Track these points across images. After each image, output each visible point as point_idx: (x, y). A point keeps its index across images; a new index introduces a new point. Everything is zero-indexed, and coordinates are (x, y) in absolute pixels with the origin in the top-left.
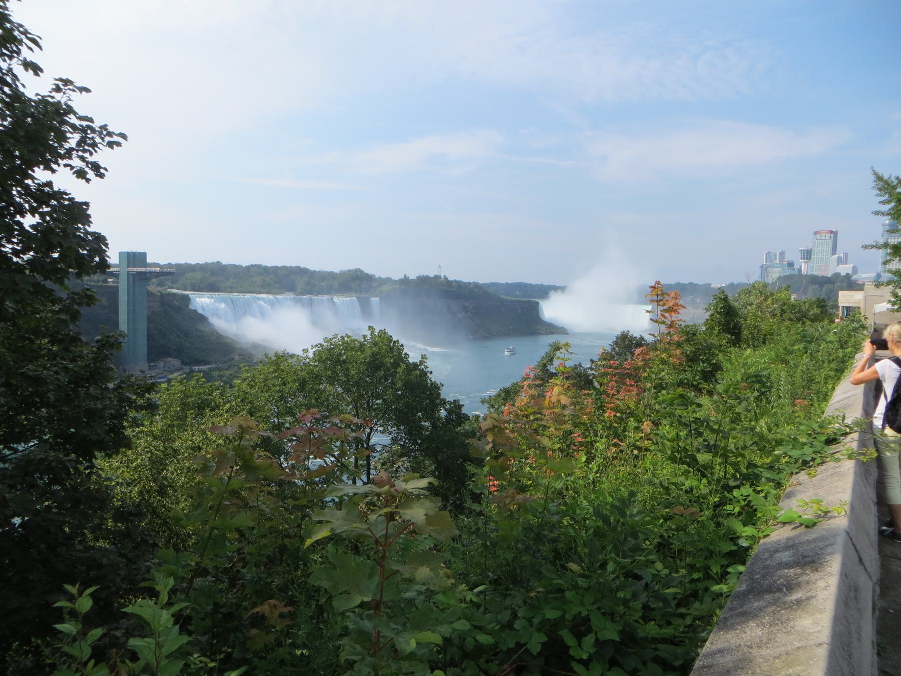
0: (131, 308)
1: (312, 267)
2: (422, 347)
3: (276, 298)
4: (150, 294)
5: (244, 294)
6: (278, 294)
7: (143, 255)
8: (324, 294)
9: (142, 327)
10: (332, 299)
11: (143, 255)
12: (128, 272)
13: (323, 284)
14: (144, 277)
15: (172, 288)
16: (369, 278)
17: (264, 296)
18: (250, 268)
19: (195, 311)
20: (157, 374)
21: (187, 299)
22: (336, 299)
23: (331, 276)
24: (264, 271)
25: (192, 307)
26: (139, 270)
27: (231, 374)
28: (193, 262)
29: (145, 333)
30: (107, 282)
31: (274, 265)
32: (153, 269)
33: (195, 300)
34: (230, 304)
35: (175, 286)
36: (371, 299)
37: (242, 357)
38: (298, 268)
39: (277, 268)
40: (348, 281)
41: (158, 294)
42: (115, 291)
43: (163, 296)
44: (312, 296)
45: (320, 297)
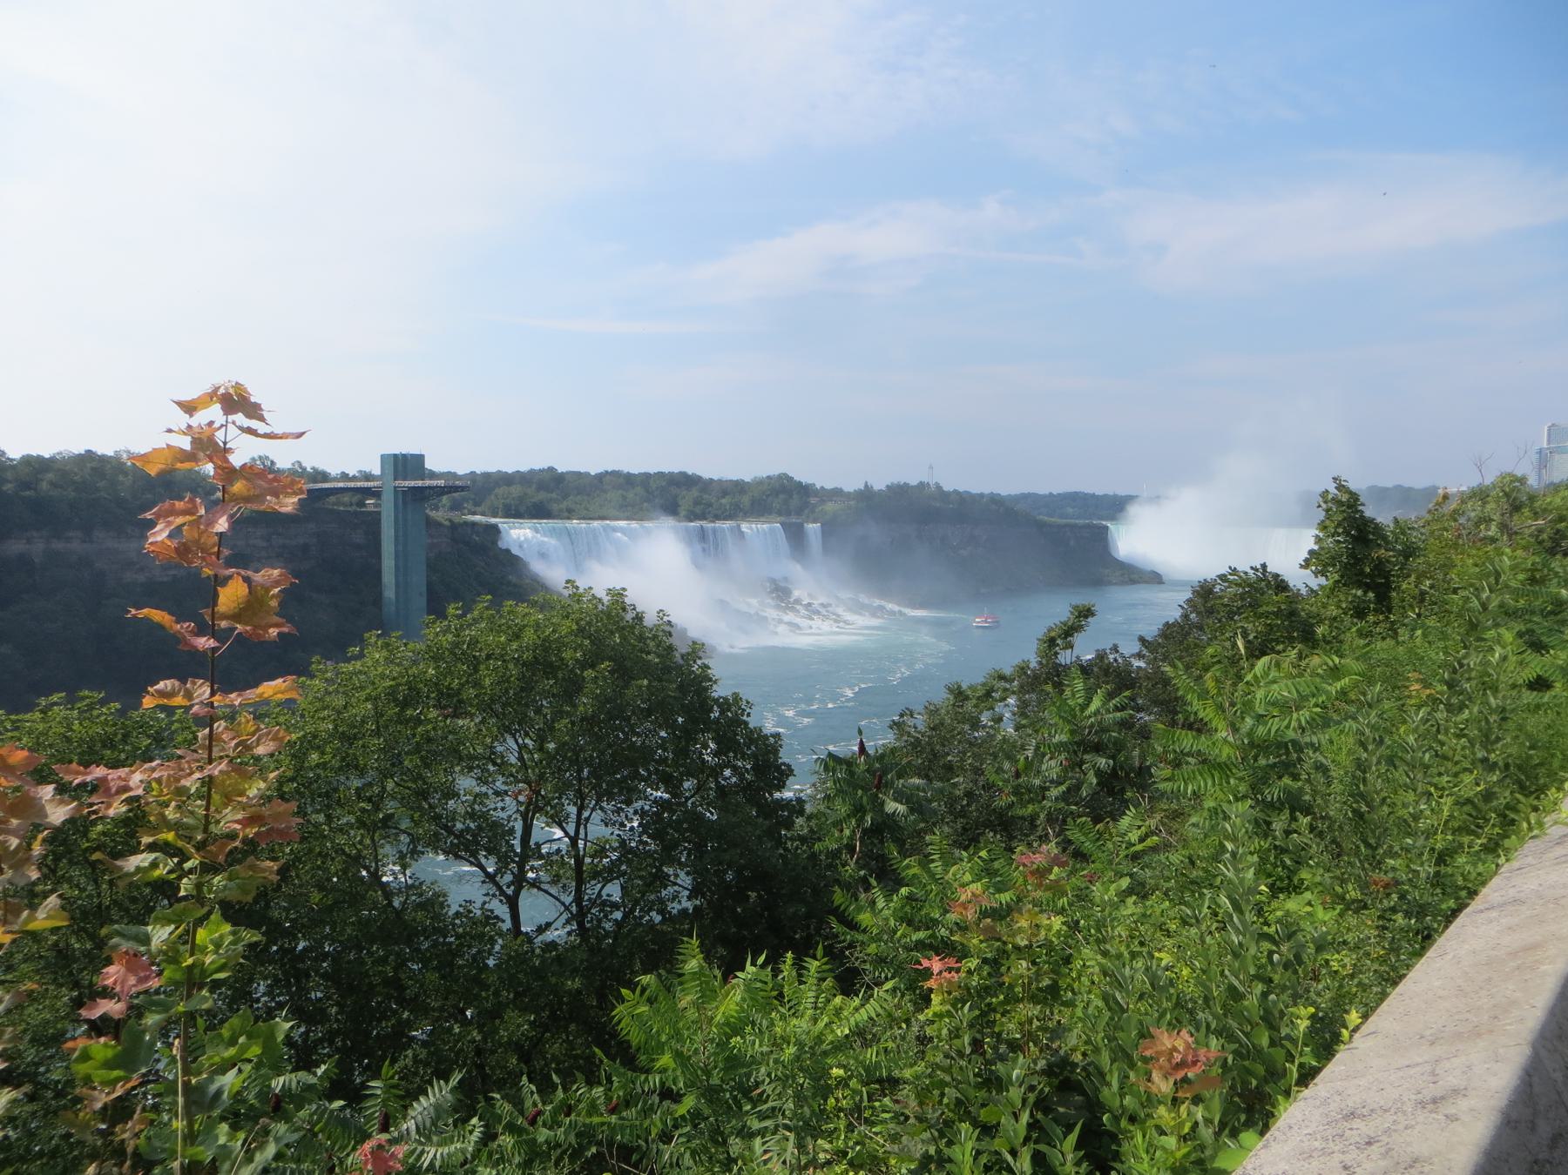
0: (401, 548)
1: (706, 473)
2: (896, 608)
4: (430, 523)
7: (420, 459)
9: (419, 580)
10: (739, 526)
11: (420, 459)
13: (724, 501)
14: (419, 496)
16: (805, 490)
17: (622, 523)
19: (508, 551)
21: (495, 530)
22: (745, 527)
23: (739, 487)
24: (623, 481)
26: (412, 483)
28: (510, 469)
30: (364, 505)
31: (643, 471)
32: (434, 483)
33: (508, 533)
38: (683, 475)
39: (647, 476)
40: (768, 496)
41: (447, 523)
42: (374, 520)
43: (454, 526)
44: (704, 523)
45: (718, 524)
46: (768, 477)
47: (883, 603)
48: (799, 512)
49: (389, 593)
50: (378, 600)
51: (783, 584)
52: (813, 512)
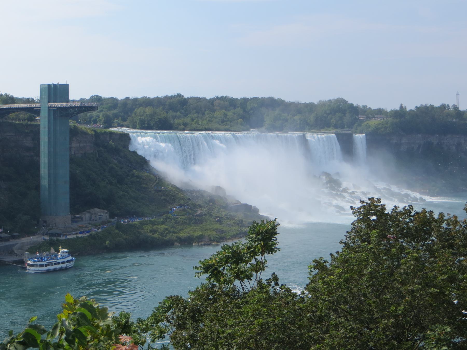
2: (418, 195)
3: (234, 136)
5: (193, 132)
6: (239, 131)
8: (296, 130)
10: (304, 136)
12: (49, 107)
13: (296, 117)
15: (122, 126)
18: (212, 101)
19: (135, 153)
20: (80, 227)
21: (126, 138)
22: (309, 136)
23: (310, 107)
25: (131, 148)
26: (59, 105)
27: (166, 229)
29: (68, 179)
33: (135, 139)
34: (177, 143)
35: (125, 123)
36: (354, 135)
37: (183, 207)
40: (328, 114)
46: (330, 101)
47: (409, 192)
48: (350, 126)
49: (45, 182)
50: (38, 187)
51: (335, 177)
52: (360, 125)
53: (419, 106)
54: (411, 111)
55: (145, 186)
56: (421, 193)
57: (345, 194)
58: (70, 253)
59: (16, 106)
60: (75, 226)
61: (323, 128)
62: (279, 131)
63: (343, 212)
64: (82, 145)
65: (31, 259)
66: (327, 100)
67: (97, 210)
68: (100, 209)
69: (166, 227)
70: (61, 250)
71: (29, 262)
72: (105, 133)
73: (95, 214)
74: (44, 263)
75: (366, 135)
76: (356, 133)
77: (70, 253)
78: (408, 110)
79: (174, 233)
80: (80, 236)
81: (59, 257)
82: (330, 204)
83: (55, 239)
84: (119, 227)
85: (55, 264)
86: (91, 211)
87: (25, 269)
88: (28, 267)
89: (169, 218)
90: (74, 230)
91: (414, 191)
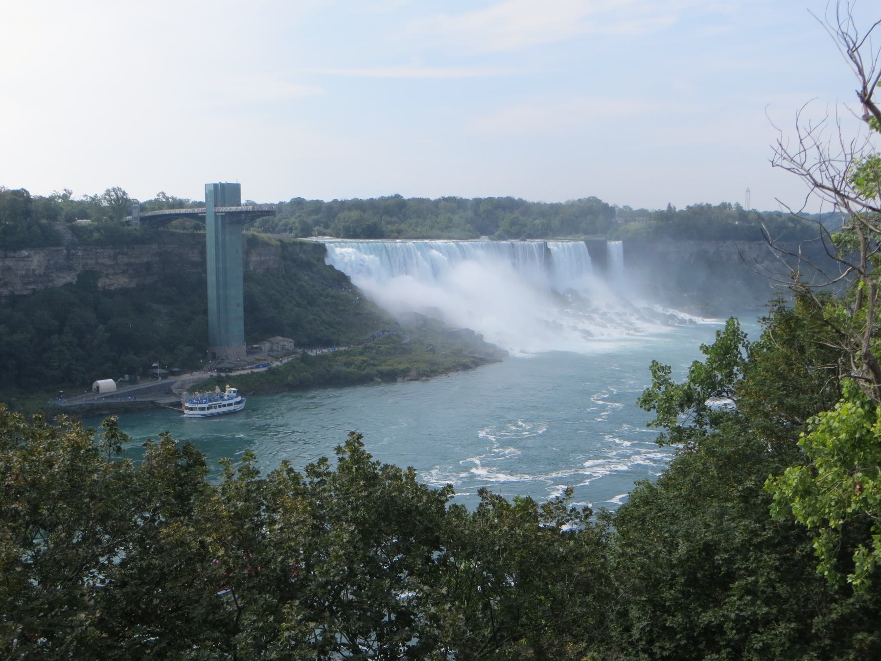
2: (687, 316)
3: (458, 245)
10: (545, 244)
17: (440, 242)
19: (331, 267)
21: (321, 250)
22: (551, 245)
23: (555, 209)
25: (328, 262)
27: (364, 361)
46: (580, 200)
49: (212, 305)
50: (205, 312)
53: (691, 205)
54: (681, 211)
55: (341, 308)
56: (690, 312)
57: (594, 316)
58: (239, 393)
59: (183, 211)
60: (251, 358)
61: (570, 234)
62: (515, 238)
63: (589, 338)
64: (263, 258)
65: (191, 402)
66: (576, 199)
67: (280, 338)
68: (283, 336)
69: (365, 358)
70: (228, 389)
71: (187, 405)
72: (295, 243)
73: (277, 343)
74: (206, 406)
75: (624, 243)
76: (611, 239)
77: (239, 393)
78: (677, 210)
79: (374, 365)
80: (255, 370)
81: (226, 398)
82: (575, 328)
83: (223, 375)
84: (305, 359)
85: (220, 406)
86: (273, 339)
87: (183, 413)
88: (186, 411)
89: (369, 347)
90: (249, 364)
91: (682, 311)
